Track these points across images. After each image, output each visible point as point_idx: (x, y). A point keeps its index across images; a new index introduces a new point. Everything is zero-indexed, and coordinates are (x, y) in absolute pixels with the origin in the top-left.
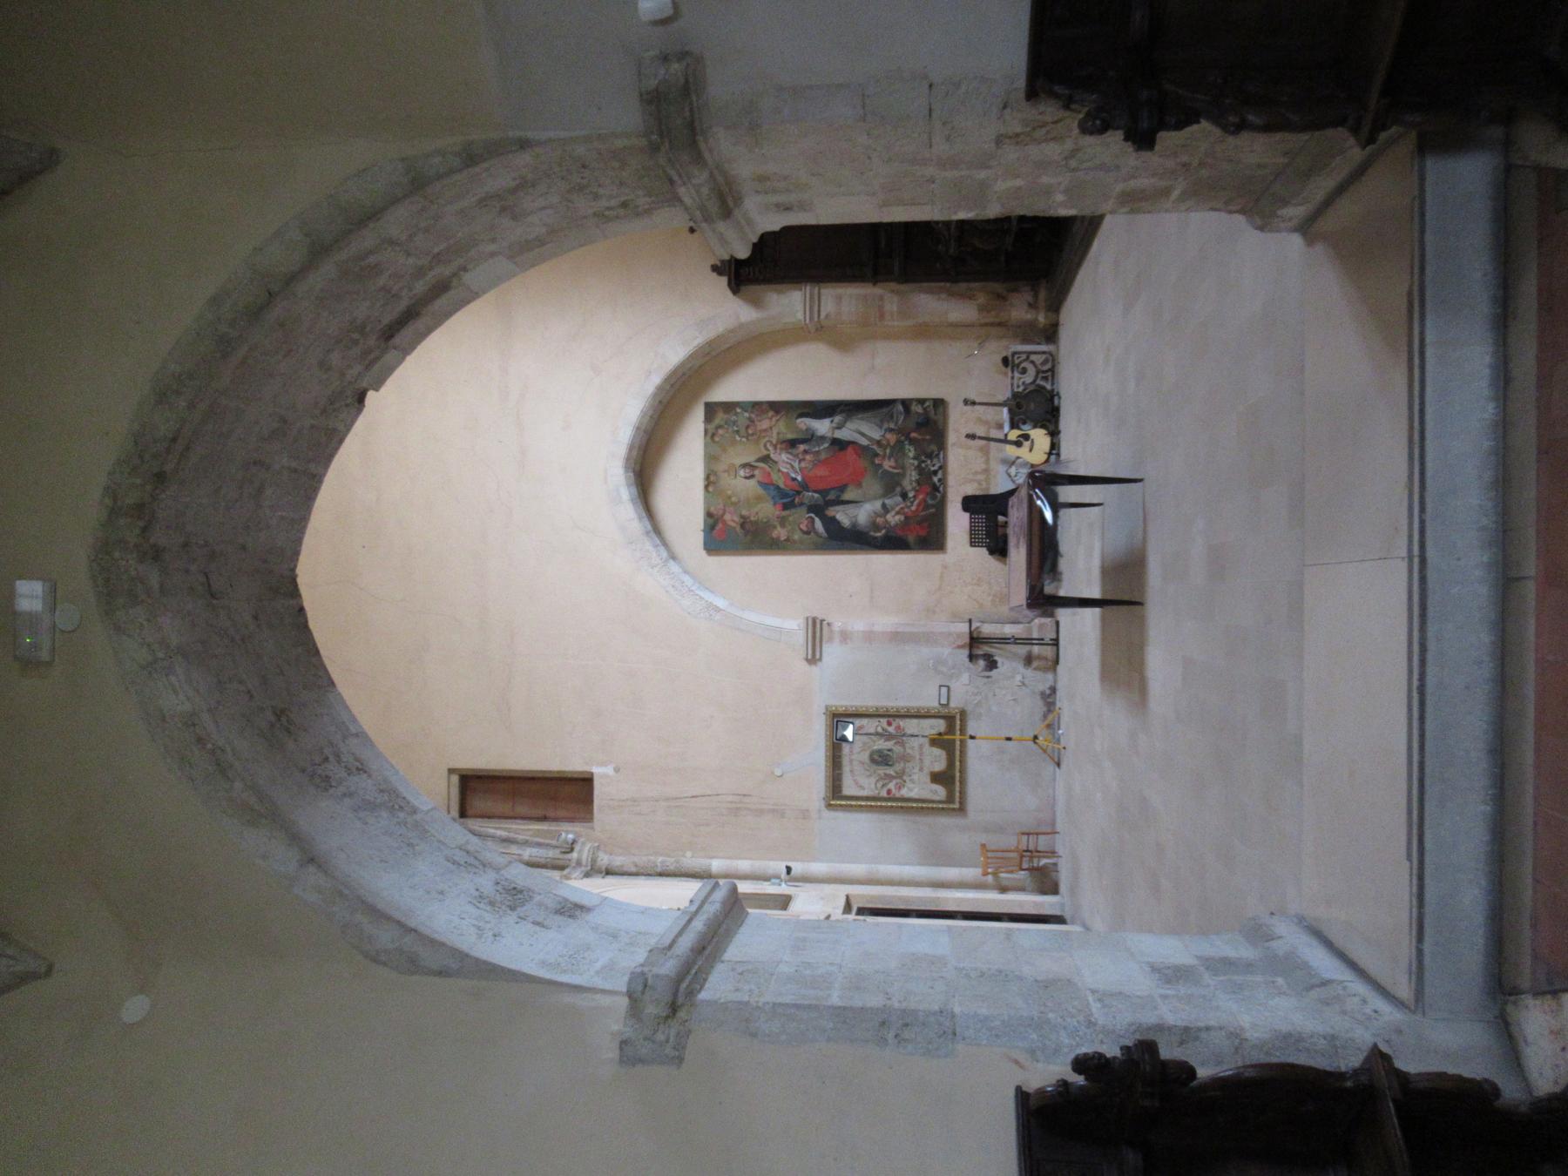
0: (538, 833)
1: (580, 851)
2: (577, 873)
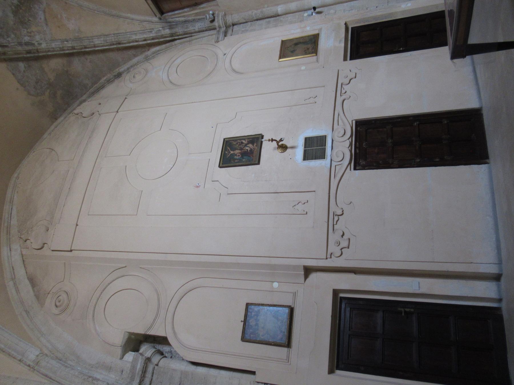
0: (197, 14)
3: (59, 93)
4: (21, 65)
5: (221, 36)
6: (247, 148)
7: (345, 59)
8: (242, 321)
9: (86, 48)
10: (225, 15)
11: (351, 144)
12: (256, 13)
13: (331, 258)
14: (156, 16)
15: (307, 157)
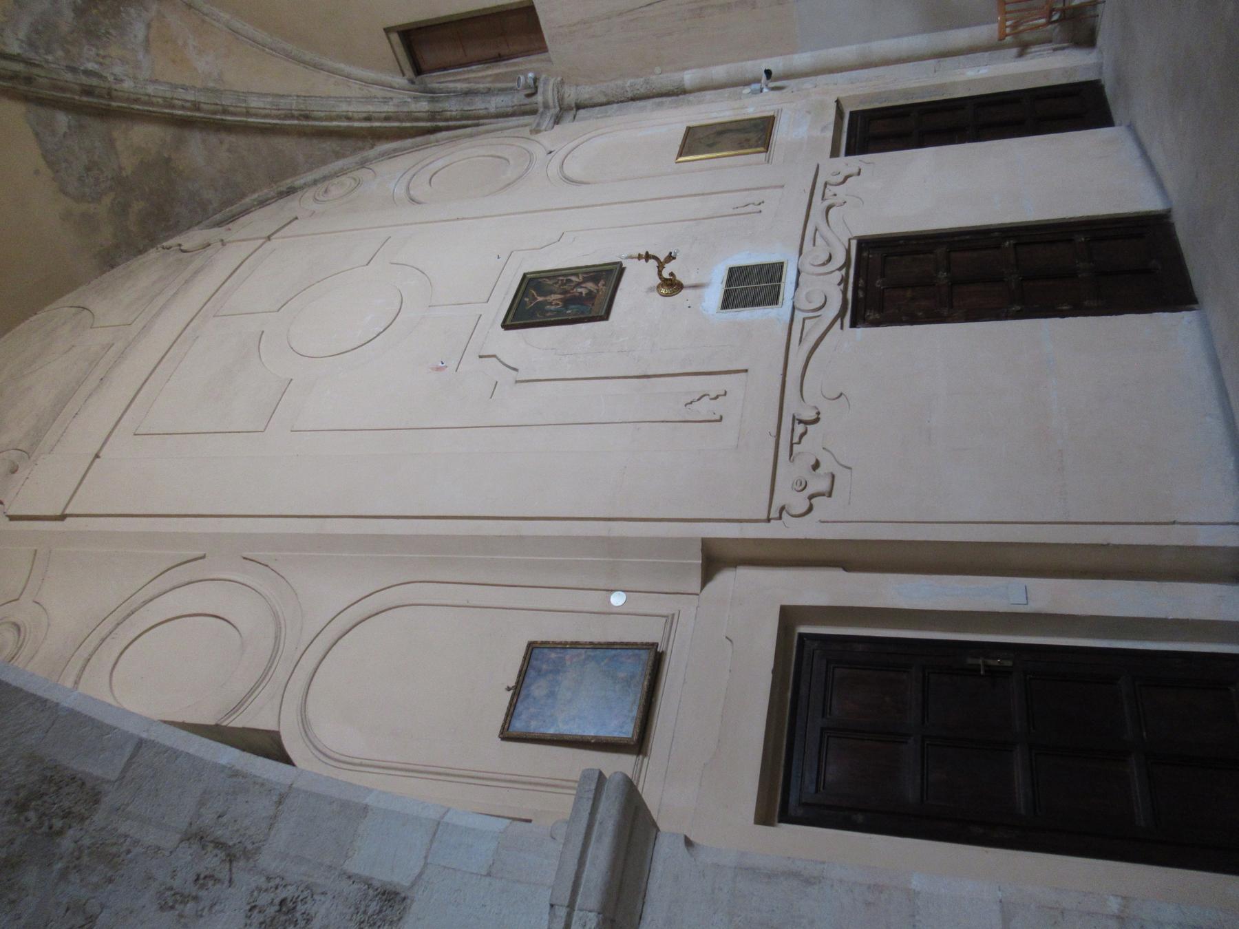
0: (497, 78)
1: (544, 93)
2: (547, 122)
3: (138, 206)
4: (63, 120)
5: (547, 122)
7: (835, 153)
8: (509, 689)
9: (225, 112)
10: (562, 82)
11: (844, 280)
12: (637, 84)
13: (780, 518)
14: (404, 75)
15: (728, 302)
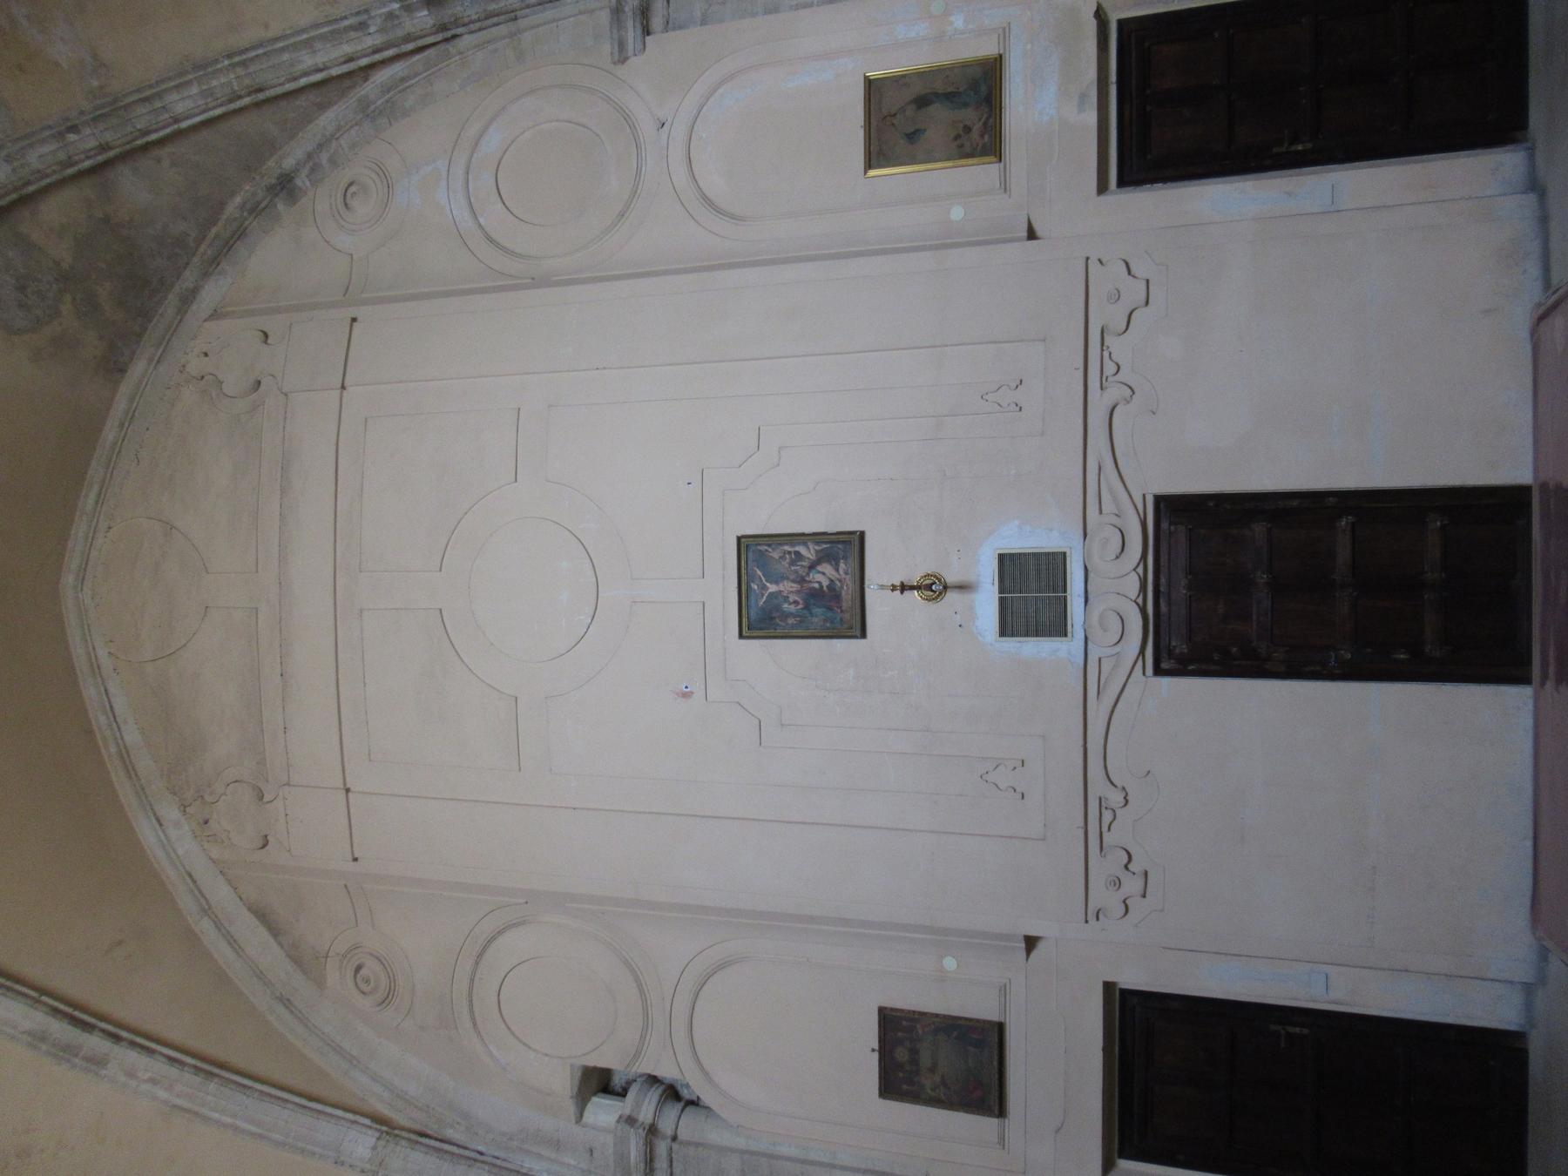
6: (819, 577)
7: (1102, 188)
